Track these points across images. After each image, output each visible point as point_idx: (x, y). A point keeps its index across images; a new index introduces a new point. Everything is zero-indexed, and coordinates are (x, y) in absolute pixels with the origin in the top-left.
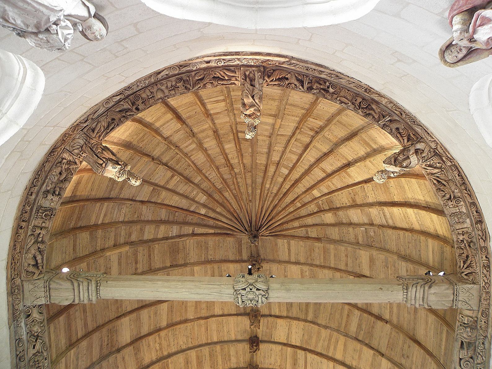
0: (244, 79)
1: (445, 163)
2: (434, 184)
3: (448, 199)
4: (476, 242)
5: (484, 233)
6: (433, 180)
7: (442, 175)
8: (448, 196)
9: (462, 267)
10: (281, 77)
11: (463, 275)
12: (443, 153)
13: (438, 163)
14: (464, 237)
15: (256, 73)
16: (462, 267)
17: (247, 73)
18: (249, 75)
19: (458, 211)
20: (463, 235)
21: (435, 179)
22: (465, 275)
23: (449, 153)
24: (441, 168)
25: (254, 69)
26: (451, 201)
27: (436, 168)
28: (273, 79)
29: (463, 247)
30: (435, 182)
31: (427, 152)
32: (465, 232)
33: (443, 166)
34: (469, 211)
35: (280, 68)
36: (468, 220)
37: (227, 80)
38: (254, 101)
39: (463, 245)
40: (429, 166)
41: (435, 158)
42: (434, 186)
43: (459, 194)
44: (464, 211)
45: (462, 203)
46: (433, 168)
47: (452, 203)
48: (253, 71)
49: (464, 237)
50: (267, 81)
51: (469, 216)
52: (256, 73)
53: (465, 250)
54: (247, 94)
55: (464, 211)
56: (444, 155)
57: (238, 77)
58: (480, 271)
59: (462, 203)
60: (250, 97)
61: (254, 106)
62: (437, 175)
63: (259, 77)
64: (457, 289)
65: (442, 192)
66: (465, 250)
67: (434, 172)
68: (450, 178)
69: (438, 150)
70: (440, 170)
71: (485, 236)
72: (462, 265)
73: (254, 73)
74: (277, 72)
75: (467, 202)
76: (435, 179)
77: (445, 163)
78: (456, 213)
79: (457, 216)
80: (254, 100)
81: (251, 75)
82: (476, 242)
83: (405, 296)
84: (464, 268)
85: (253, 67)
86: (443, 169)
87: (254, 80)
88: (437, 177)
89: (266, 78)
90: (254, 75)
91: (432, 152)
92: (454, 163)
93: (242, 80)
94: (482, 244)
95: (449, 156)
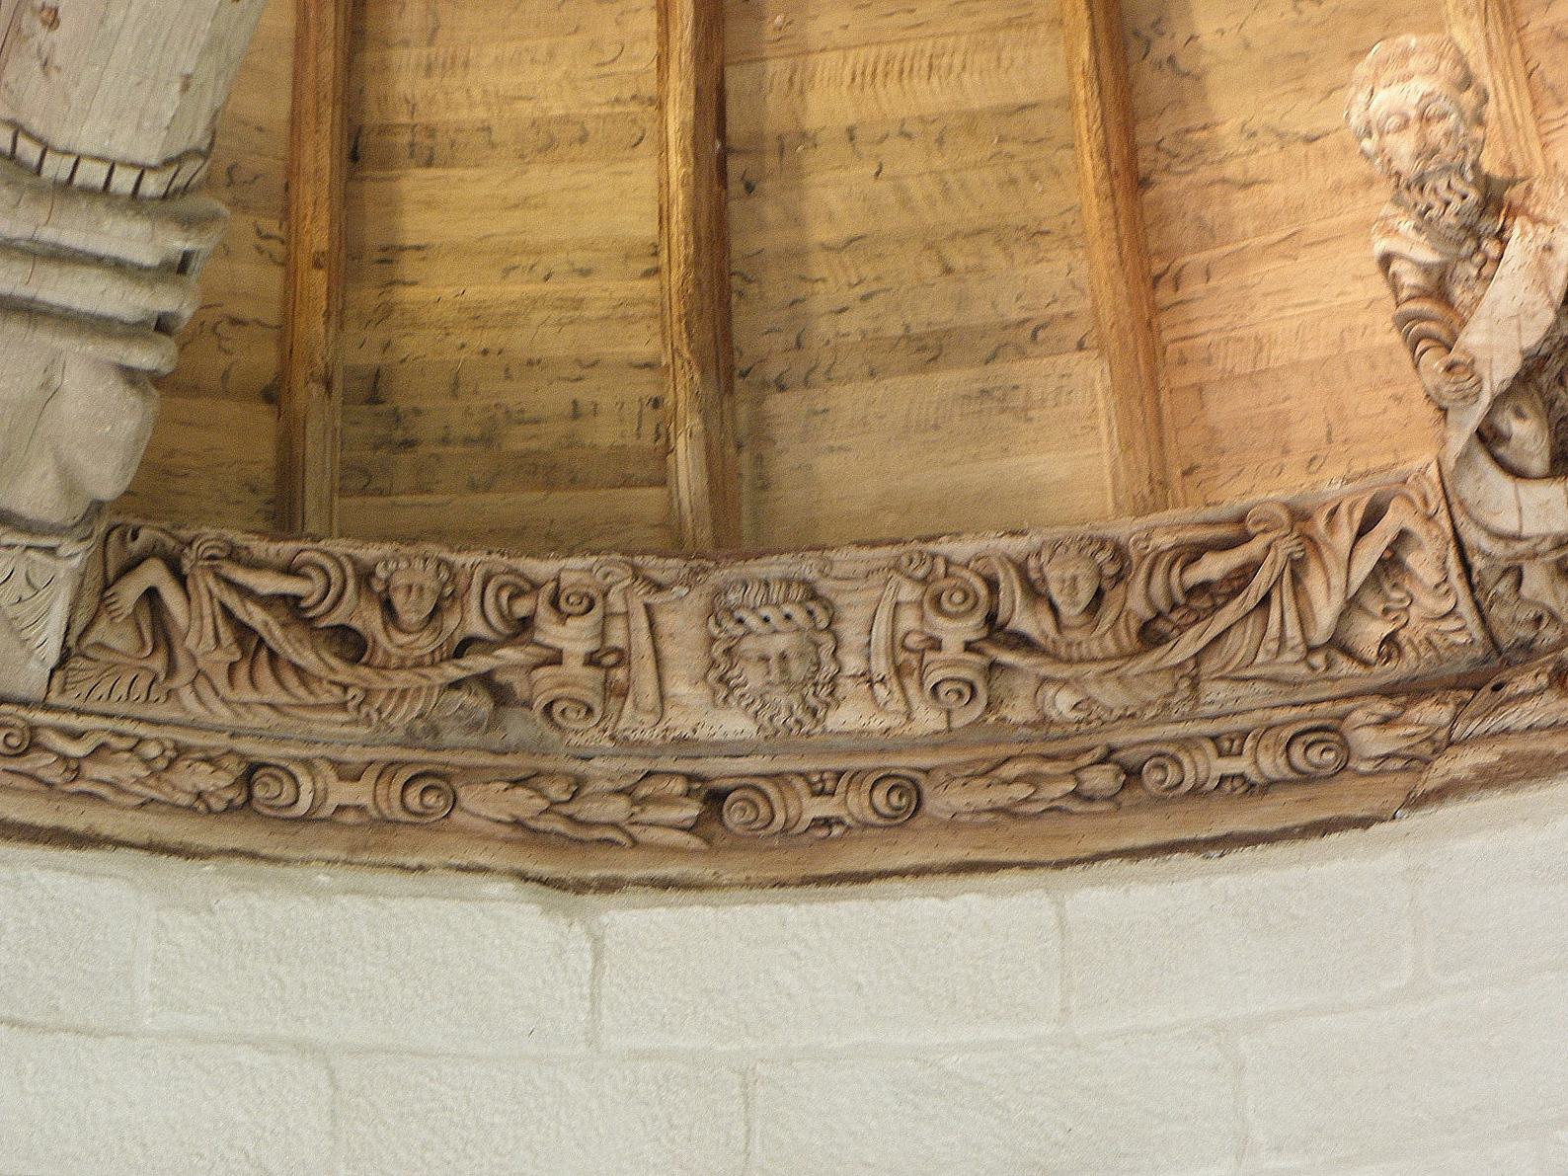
1: (1387, 692)
2: (1193, 553)
3: (991, 619)
4: (495, 739)
5: (597, 834)
6: (1235, 558)
7: (1273, 646)
8: (1026, 621)
9: (240, 576)
11: (154, 574)
12: (1492, 723)
13: (1390, 639)
14: (574, 666)
16: (240, 576)
19: (853, 663)
20: (592, 660)
21: (1245, 574)
22: (152, 595)
23: (1489, 779)
24: (1339, 644)
26: (969, 647)
27: (1352, 605)
29: (451, 622)
30: (1213, 567)
31: (1550, 602)
32: (620, 674)
33: (1344, 666)
34: (831, 751)
36: (735, 724)
39: (476, 627)
40: (1391, 564)
41: (1461, 639)
42: (1164, 541)
43: (1018, 711)
44: (849, 716)
45: (929, 719)
46: (1365, 583)
47: (953, 644)
49: (574, 666)
51: (772, 742)
53: (425, 643)
55: (849, 716)
56: (1476, 727)
58: (194, 726)
59: (929, 719)
62: (1283, 609)
64: (51, 551)
65: (1085, 595)
66: (425, 643)
67: (1315, 583)
68: (1217, 693)
69: (1539, 692)
70: (1319, 637)
71: (570, 850)
72: (268, 583)
75: (926, 761)
76: (1245, 574)
77: (1387, 692)
78: (830, 645)
79: (801, 655)
82: (495, 739)
83: (92, 174)
84: (232, 601)
86: (1318, 660)
88: (1265, 602)
91: (1525, 633)
92: (1364, 767)
94: (486, 803)
95: (1462, 763)
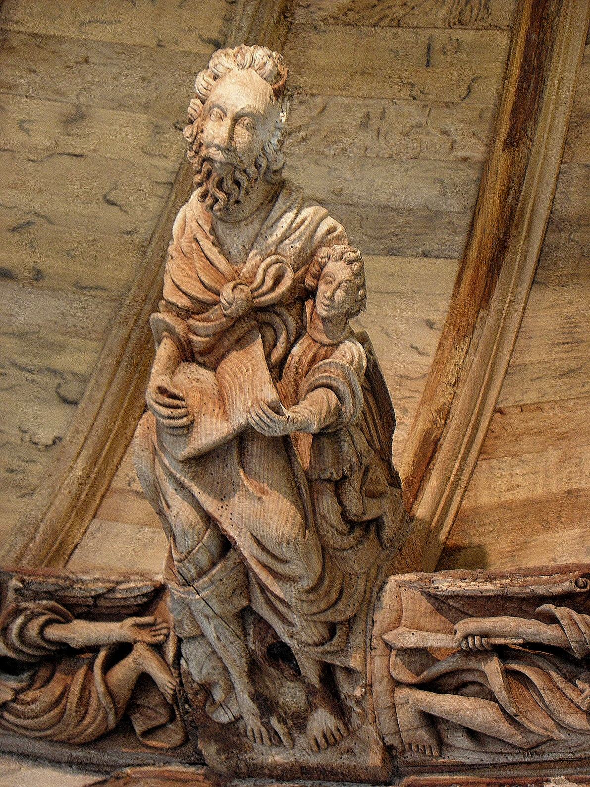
0: (340, 676)
10: (55, 688)
15: (252, 723)
17: (322, 720)
18: (312, 707)
25: (276, 757)
28: (108, 666)
35: (82, 754)
37: (503, 653)
38: (210, 504)
48: (275, 740)
50: (158, 648)
52: (252, 723)
54: (279, 568)
57: (398, 684)
60: (246, 547)
61: (200, 461)
63: (218, 695)
73: (267, 725)
74: (92, 725)
80: (209, 520)
81: (291, 696)
85: (282, 767)
87: (253, 670)
89: (164, 679)
90: (266, 705)
93: (354, 661)
